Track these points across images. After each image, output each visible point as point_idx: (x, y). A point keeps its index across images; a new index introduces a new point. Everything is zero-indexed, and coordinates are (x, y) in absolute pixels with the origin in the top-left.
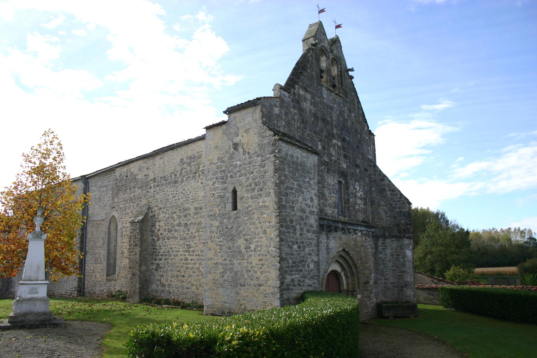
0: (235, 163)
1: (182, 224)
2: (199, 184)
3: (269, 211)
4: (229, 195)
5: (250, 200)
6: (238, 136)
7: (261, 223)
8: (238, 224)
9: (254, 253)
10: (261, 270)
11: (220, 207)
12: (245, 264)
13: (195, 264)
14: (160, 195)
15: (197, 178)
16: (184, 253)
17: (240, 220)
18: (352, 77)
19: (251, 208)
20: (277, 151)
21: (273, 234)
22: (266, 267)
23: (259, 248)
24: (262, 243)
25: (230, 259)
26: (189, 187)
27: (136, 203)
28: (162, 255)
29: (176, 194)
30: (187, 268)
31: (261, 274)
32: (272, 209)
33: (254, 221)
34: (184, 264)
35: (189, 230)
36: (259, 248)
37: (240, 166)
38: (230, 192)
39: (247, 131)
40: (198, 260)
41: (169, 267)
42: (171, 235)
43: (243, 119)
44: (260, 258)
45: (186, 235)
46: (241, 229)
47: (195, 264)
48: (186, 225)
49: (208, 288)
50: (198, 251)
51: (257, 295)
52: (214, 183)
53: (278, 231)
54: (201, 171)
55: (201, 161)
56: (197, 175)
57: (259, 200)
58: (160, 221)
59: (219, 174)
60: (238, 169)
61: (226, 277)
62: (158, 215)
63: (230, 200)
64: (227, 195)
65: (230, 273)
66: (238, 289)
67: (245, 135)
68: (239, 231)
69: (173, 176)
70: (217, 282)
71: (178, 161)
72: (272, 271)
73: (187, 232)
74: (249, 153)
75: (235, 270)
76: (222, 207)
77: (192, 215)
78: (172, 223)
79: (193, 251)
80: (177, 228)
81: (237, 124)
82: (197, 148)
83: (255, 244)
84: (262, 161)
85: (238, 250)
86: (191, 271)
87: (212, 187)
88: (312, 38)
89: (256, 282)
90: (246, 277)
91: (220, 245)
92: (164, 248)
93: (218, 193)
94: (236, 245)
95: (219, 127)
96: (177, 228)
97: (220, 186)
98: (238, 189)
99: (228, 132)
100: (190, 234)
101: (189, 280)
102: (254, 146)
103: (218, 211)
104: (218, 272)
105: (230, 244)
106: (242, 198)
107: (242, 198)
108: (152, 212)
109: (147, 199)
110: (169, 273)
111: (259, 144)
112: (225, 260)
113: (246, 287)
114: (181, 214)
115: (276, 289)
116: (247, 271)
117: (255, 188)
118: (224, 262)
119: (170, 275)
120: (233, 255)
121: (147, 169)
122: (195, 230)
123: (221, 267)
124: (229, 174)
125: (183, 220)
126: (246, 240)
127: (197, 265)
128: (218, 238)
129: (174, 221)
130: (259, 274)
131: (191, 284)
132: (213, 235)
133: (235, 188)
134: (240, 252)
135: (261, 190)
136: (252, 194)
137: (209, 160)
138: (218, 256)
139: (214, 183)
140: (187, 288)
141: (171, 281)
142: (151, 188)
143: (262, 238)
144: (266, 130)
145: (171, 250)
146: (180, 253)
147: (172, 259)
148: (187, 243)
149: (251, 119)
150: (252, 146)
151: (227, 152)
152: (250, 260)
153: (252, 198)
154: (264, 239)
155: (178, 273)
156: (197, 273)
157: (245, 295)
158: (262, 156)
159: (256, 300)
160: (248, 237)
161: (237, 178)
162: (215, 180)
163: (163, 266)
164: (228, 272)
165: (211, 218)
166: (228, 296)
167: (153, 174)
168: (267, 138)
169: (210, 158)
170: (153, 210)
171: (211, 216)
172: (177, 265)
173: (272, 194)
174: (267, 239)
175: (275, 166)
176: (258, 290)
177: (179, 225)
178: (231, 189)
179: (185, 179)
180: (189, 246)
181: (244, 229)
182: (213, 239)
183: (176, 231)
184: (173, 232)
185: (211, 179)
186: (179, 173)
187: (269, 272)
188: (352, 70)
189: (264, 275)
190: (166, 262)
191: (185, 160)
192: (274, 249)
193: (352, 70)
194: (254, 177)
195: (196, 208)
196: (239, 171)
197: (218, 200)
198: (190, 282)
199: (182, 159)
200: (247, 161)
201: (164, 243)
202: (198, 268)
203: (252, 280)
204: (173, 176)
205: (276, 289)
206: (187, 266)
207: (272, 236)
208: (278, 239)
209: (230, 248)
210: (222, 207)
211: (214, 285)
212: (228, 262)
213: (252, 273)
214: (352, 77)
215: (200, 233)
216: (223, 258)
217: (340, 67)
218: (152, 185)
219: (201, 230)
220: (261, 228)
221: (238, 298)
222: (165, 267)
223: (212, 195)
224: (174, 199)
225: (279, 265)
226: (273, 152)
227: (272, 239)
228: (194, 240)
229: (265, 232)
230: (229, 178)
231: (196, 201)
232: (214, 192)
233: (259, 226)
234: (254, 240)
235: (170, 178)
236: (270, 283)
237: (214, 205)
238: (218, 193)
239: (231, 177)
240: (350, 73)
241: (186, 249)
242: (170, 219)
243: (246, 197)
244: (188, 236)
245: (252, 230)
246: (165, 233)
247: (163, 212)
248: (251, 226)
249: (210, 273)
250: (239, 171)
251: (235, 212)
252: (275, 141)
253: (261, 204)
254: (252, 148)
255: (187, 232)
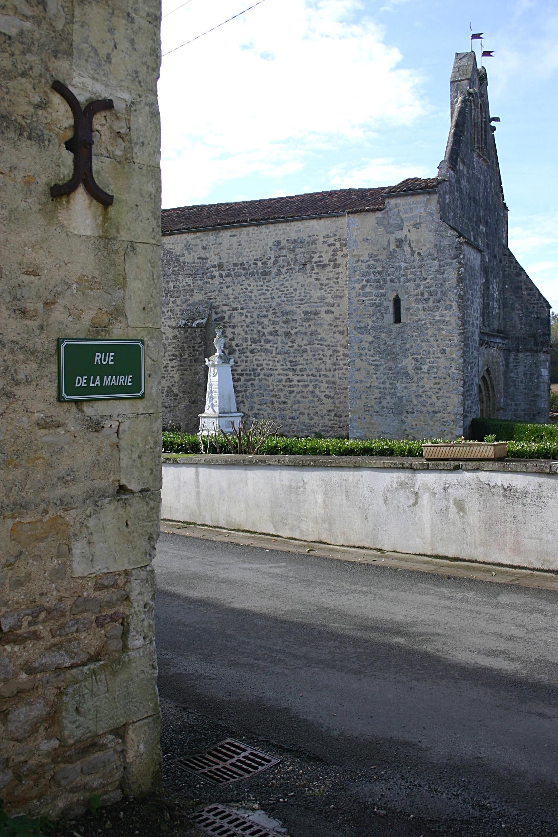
0: (398, 264)
1: (279, 333)
2: (312, 280)
3: (449, 328)
4: (391, 305)
5: (421, 312)
6: (402, 229)
7: (437, 340)
8: (403, 340)
9: (427, 375)
10: (437, 395)
11: (374, 318)
12: (414, 388)
13: (306, 386)
14: (233, 290)
15: (308, 272)
16: (286, 372)
17: (406, 336)
18: (494, 129)
19: (423, 322)
20: (461, 256)
21: (456, 354)
22: (445, 391)
23: (435, 370)
24: (440, 365)
25: (391, 381)
26: (294, 282)
27: (182, 297)
28: (242, 375)
29: (267, 290)
30: (291, 392)
31: (438, 399)
32: (454, 325)
33: (428, 337)
34: (284, 386)
35: (293, 342)
36: (435, 370)
37: (406, 268)
38: (390, 301)
39: (416, 226)
40: (311, 382)
41: (254, 390)
42: (259, 348)
43: (411, 209)
44: (437, 381)
45: (288, 348)
46: (408, 346)
47: (306, 386)
48: (287, 334)
49: (356, 416)
50: (311, 370)
51: (431, 423)
52: (364, 287)
53: (461, 351)
54: (315, 263)
55: (316, 248)
56: (308, 267)
57: (435, 314)
58: (234, 327)
59: (372, 276)
60: (402, 272)
61: (384, 403)
62: (230, 318)
63: (391, 310)
64: (385, 304)
65: (392, 398)
66: (403, 417)
67: (413, 230)
68: (404, 348)
69: (260, 264)
70: (371, 409)
71: (271, 244)
72: (452, 396)
73: (290, 344)
74: (419, 254)
75: (398, 395)
76: (378, 318)
77: (299, 321)
78: (259, 331)
79: (301, 370)
80: (270, 338)
81: (401, 214)
82: (308, 230)
83: (429, 365)
84: (440, 266)
85: (403, 371)
86: (299, 396)
87: (361, 291)
88: (466, 81)
89: (431, 409)
90: (415, 402)
91: (376, 365)
92: (244, 364)
93: (370, 300)
94: (399, 365)
95: (371, 214)
96: (270, 338)
97: (374, 292)
98: (404, 299)
99: (386, 222)
100: (295, 346)
101: (295, 407)
102: (428, 246)
103: (371, 324)
104: (373, 397)
105: (391, 364)
106: (408, 309)
107: (408, 309)
108: (216, 313)
109: (206, 294)
110: (256, 399)
111: (436, 245)
112: (383, 383)
113: (415, 414)
114: (278, 319)
115: (458, 417)
116: (417, 396)
117: (429, 299)
118: (382, 386)
119: (257, 402)
120: (395, 377)
121: (204, 248)
122: (305, 342)
123: (377, 391)
124: (388, 278)
125: (283, 327)
126: (416, 360)
127: (311, 388)
128: (372, 356)
129: (263, 328)
130: (434, 399)
131: (298, 412)
132: (364, 352)
133: (397, 296)
134: (407, 374)
135: (439, 301)
136: (425, 305)
137: (355, 256)
138: (372, 378)
139: (364, 287)
140: (292, 418)
141: (259, 410)
142: (213, 277)
143: (439, 358)
144: (446, 227)
145: (259, 368)
146: (276, 372)
147: (260, 380)
148: (291, 359)
149: (423, 211)
150: (425, 245)
151: (384, 249)
152: (421, 383)
153: (424, 309)
154: (442, 360)
155: (274, 399)
156: (311, 399)
157: (414, 424)
158: (439, 261)
159: (429, 428)
160: (419, 357)
161: (401, 284)
162: (364, 283)
163: (243, 389)
164: (389, 398)
165: (359, 330)
166: (389, 425)
167: (217, 258)
168: (448, 238)
169: (355, 253)
170: (219, 310)
171: (360, 328)
172: (271, 388)
173: (454, 308)
174: (446, 359)
175: (459, 274)
176: (432, 417)
177: (274, 333)
178: (392, 296)
179: (284, 270)
180: (294, 364)
181: (412, 347)
182: (363, 358)
183: (268, 341)
184: (262, 343)
185: (358, 281)
186: (272, 261)
187: (450, 397)
188: (497, 119)
189: (441, 400)
190: (249, 383)
191: (284, 243)
192: (457, 371)
193: (497, 119)
194: (427, 285)
195: (306, 313)
196: (403, 275)
197: (371, 309)
198: (296, 411)
199: (279, 242)
200: (417, 263)
201: (243, 358)
202: (312, 392)
203: (424, 406)
204: (260, 264)
205: (458, 417)
206: (292, 389)
207: (454, 356)
208: (462, 360)
209: (390, 369)
210: (378, 318)
211: (367, 413)
212: (387, 385)
213: (424, 397)
214: (494, 129)
215: (315, 346)
216: (381, 381)
217: (484, 116)
218: (217, 274)
219: (316, 342)
220: (438, 347)
221: (403, 428)
222: (246, 391)
223: (361, 302)
224: (263, 296)
225: (462, 389)
226: (456, 257)
227: (453, 359)
228: (305, 355)
229: (444, 352)
230: (389, 283)
231: (307, 303)
232: (364, 299)
233: (435, 344)
234: (428, 361)
235: (252, 266)
236: (450, 409)
237: (364, 315)
238: (370, 300)
239: (392, 281)
240: (493, 123)
241: (289, 367)
242: (256, 325)
243: (415, 308)
244: (291, 349)
245: (425, 348)
246: (245, 344)
247: (241, 314)
248: (423, 344)
249: (360, 399)
250: (403, 275)
251: (397, 325)
252: (460, 243)
253: (438, 318)
254: (424, 249)
255: (290, 344)
